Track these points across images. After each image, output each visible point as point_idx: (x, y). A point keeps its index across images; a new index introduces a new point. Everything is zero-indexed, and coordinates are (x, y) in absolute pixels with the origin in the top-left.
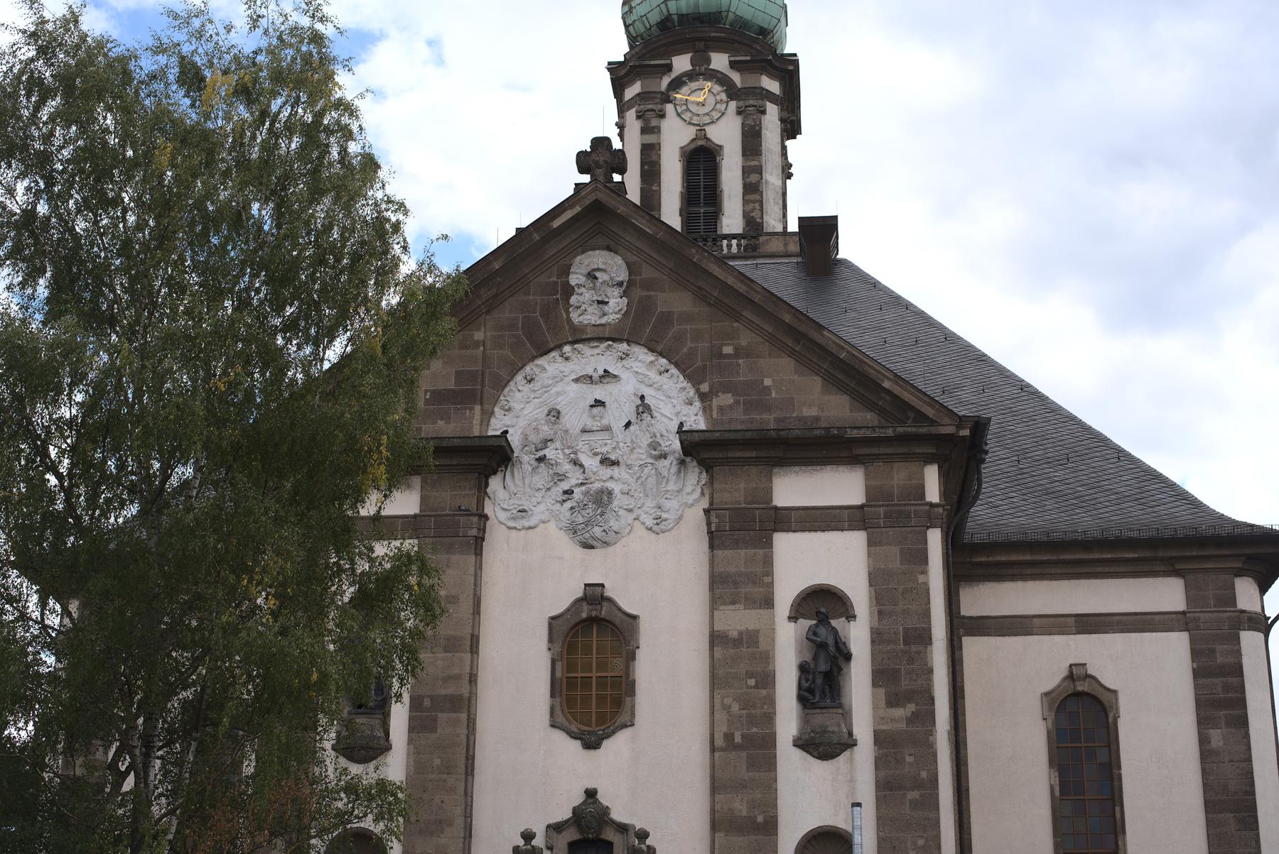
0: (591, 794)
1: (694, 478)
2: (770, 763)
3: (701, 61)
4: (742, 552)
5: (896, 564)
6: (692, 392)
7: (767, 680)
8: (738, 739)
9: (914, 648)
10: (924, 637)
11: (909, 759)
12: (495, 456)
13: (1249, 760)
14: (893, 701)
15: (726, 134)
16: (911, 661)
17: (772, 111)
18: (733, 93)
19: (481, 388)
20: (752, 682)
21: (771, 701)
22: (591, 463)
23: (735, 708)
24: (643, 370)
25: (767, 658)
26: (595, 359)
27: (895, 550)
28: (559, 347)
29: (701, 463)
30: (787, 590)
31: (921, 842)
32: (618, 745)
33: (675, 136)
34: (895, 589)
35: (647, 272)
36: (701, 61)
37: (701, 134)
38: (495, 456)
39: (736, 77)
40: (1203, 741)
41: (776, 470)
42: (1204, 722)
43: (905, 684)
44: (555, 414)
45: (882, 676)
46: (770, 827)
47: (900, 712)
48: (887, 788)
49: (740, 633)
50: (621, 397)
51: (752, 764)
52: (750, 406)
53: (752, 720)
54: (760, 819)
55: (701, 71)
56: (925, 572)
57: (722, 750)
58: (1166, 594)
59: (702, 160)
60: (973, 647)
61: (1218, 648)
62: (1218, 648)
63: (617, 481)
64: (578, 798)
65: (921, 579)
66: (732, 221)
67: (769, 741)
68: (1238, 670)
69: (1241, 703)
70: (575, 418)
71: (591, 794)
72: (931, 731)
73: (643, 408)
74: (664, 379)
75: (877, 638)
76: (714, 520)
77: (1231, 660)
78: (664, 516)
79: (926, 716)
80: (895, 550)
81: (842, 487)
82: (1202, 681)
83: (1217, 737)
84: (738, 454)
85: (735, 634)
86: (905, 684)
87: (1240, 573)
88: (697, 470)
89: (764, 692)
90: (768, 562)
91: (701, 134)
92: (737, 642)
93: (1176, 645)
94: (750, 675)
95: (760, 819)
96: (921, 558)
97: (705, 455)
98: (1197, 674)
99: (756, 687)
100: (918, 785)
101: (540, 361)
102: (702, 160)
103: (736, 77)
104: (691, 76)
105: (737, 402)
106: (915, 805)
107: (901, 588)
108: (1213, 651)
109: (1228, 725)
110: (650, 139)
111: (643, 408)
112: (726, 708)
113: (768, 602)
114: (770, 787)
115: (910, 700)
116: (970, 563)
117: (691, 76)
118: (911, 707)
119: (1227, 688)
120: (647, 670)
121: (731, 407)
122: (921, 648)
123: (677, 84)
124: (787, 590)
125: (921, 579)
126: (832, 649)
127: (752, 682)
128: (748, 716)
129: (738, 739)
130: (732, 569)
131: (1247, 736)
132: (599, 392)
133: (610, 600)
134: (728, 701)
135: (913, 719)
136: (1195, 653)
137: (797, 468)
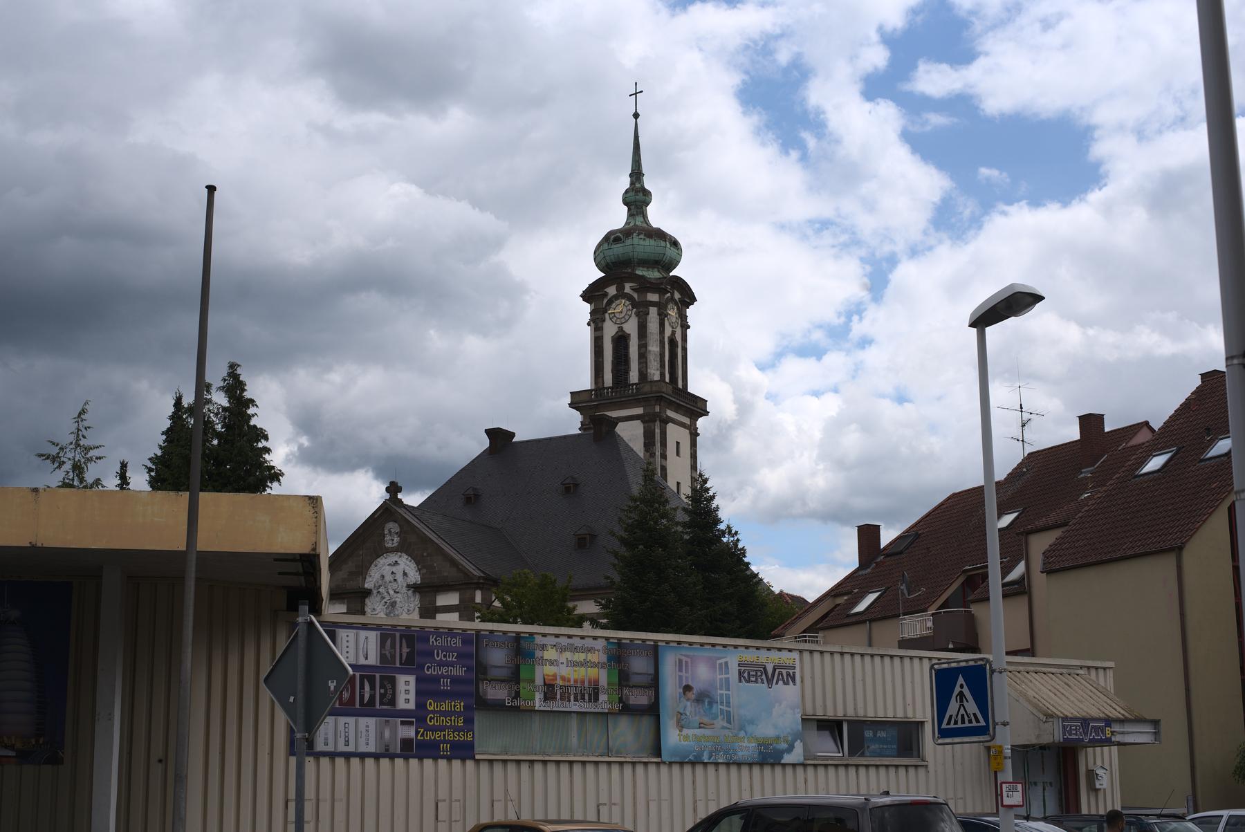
3: (620, 288)
12: (368, 593)
15: (631, 327)
17: (653, 311)
18: (634, 304)
19: (363, 571)
22: (392, 592)
26: (393, 558)
33: (610, 330)
36: (620, 288)
37: (621, 329)
38: (368, 593)
39: (635, 296)
44: (383, 577)
50: (399, 570)
55: (621, 294)
59: (621, 341)
63: (398, 598)
66: (634, 377)
70: (388, 578)
73: (405, 574)
91: (621, 329)
102: (621, 341)
103: (635, 296)
104: (616, 297)
110: (599, 334)
111: (405, 574)
117: (616, 297)
123: (610, 302)
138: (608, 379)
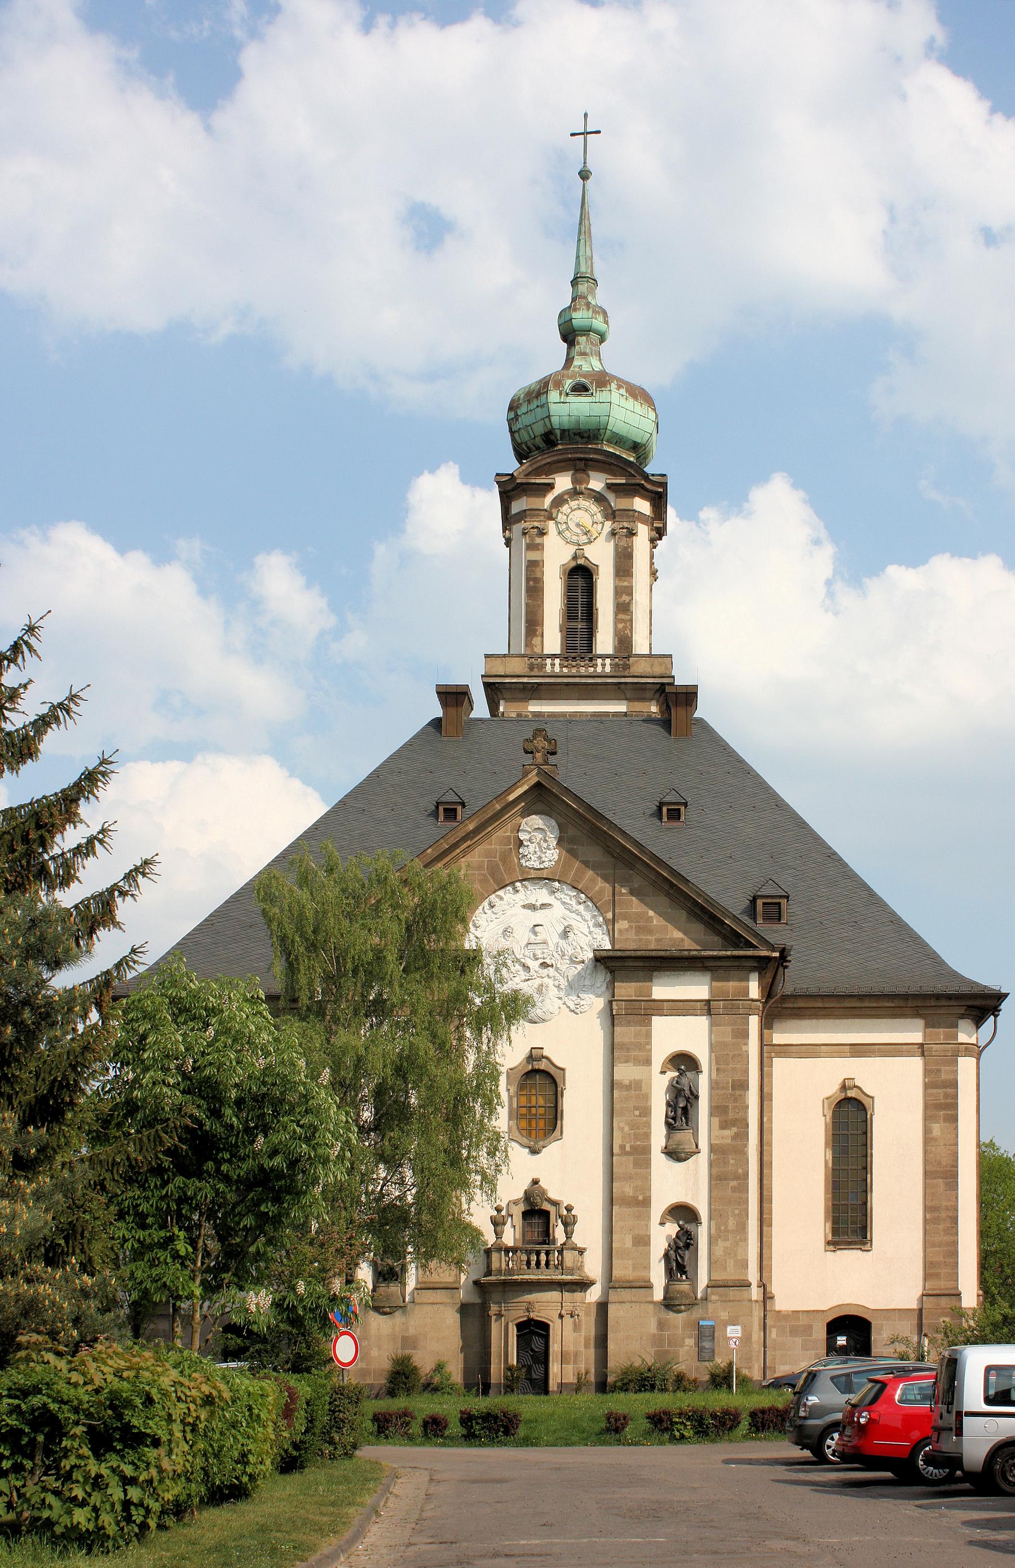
0: (535, 1182)
1: (602, 978)
2: (647, 1164)
4: (633, 1029)
5: (729, 1039)
6: (601, 919)
7: (646, 1112)
8: (628, 1149)
9: (738, 1092)
10: (744, 1086)
11: (732, 1162)
13: (957, 1144)
14: (724, 1126)
16: (736, 1100)
20: (637, 1113)
21: (648, 1125)
22: (534, 965)
23: (626, 1129)
24: (569, 902)
25: (647, 1097)
26: (539, 894)
27: (729, 1029)
28: (513, 883)
29: (607, 968)
30: (660, 1053)
31: (737, 1212)
32: (552, 1150)
34: (728, 1054)
35: (571, 832)
40: (927, 1131)
41: (655, 973)
42: (928, 1118)
43: (731, 1115)
45: (716, 1110)
46: (646, 1203)
47: (728, 1133)
48: (716, 1179)
49: (630, 1082)
51: (636, 1164)
52: (640, 930)
53: (637, 1137)
54: (641, 1198)
56: (746, 1044)
57: (618, 1155)
58: (912, 1033)
60: (780, 1065)
61: (943, 1068)
62: (943, 1068)
64: (526, 1185)
65: (744, 1048)
67: (646, 1150)
68: (954, 1084)
69: (955, 1106)
71: (535, 1182)
72: (746, 1146)
74: (581, 908)
75: (714, 1085)
76: (615, 1007)
77: (951, 1077)
78: (582, 1003)
79: (743, 1135)
80: (729, 1029)
81: (696, 988)
82: (930, 1091)
83: (936, 1129)
84: (631, 964)
85: (627, 1082)
86: (731, 1115)
87: (962, 1017)
88: (604, 972)
89: (645, 1119)
90: (649, 1035)
92: (628, 1087)
93: (915, 1065)
94: (636, 1108)
95: (641, 1198)
96: (745, 1035)
97: (610, 964)
98: (927, 1086)
99: (640, 1116)
100: (737, 1177)
101: (500, 893)
105: (631, 927)
106: (734, 1189)
107: (731, 1054)
108: (939, 1071)
109: (945, 1120)
112: (622, 1129)
113: (648, 1062)
114: (647, 1178)
115: (734, 1125)
116: (778, 1008)
118: (735, 1130)
119: (946, 1096)
120: (569, 1103)
121: (627, 930)
122: (742, 1092)
124: (660, 1053)
125: (744, 1048)
126: (687, 1092)
127: (637, 1113)
128: (635, 1134)
129: (628, 1149)
130: (626, 1040)
131: (956, 1128)
132: (538, 917)
133: (547, 1058)
134: (622, 1125)
135: (735, 1137)
136: (927, 1072)
137: (668, 973)
138: (552, 640)
